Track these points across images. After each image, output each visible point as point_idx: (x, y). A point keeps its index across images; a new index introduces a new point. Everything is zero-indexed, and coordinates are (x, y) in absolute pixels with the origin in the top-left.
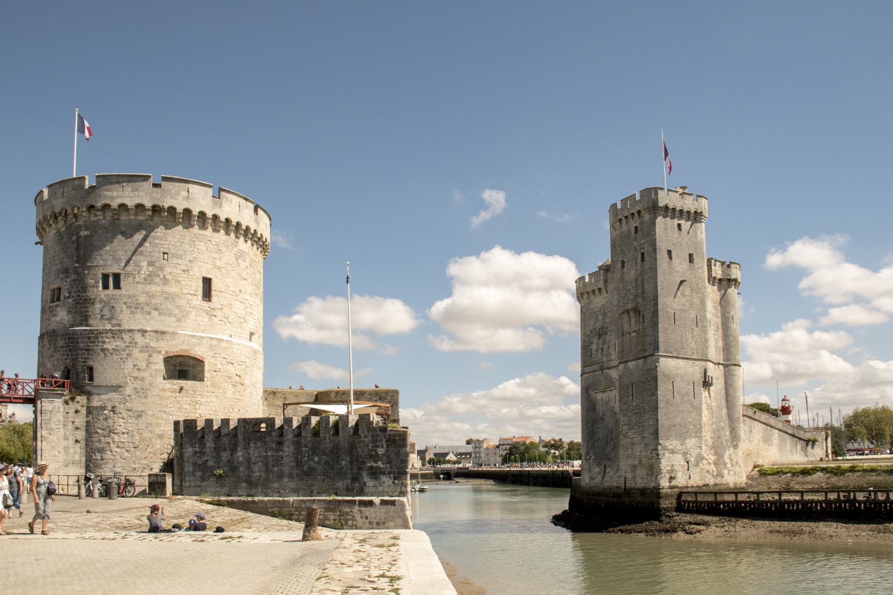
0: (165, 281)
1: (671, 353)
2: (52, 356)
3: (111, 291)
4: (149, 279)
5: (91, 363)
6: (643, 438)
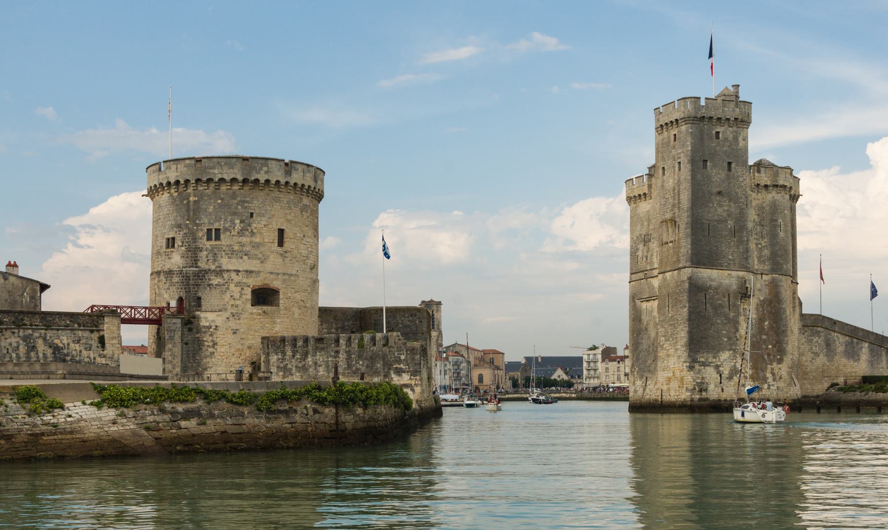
0: (253, 234)
1: (704, 265)
2: (168, 289)
3: (213, 243)
4: (241, 233)
5: (200, 294)
6: (676, 350)
